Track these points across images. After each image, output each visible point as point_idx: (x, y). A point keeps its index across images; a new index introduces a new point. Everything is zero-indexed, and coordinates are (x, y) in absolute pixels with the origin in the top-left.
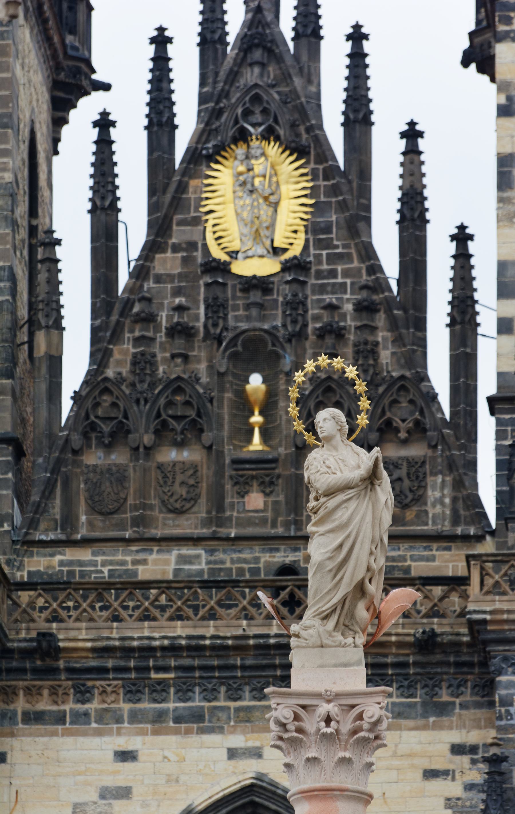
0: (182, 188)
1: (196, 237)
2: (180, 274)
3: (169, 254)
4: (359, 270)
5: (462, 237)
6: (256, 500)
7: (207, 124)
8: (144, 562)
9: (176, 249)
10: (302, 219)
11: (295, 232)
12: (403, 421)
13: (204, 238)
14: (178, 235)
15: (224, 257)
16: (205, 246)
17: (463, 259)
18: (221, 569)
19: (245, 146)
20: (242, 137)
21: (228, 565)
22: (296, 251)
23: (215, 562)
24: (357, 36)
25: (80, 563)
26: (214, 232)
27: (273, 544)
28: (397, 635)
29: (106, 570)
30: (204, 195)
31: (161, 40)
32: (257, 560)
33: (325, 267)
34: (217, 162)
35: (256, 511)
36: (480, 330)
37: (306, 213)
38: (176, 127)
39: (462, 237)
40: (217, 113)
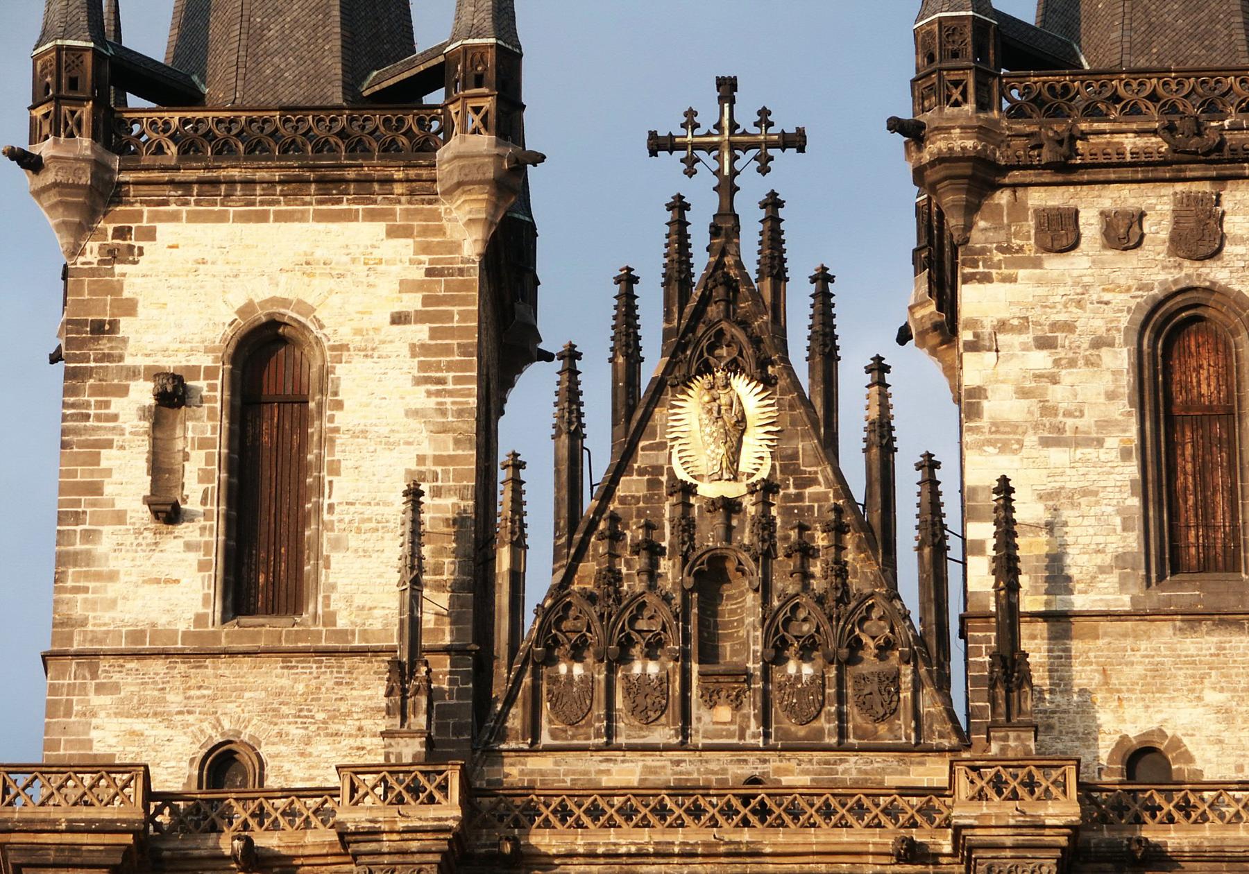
0: (648, 415)
1: (662, 461)
2: (645, 496)
3: (635, 477)
4: (827, 494)
5: (929, 464)
6: (724, 713)
7: (673, 356)
8: (608, 772)
9: (641, 472)
10: (769, 446)
11: (761, 458)
12: (873, 638)
13: (670, 462)
14: (642, 459)
15: (690, 480)
16: (671, 472)
17: (931, 485)
18: (687, 780)
19: (710, 378)
20: (706, 369)
21: (695, 776)
22: (764, 473)
23: (681, 773)
24: (823, 278)
25: (541, 773)
26: (681, 458)
27: (744, 755)
28: (874, 844)
29: (568, 779)
30: (671, 424)
31: (628, 279)
32: (724, 771)
33: (792, 490)
34: (683, 392)
35: (725, 723)
36: (949, 554)
37: (771, 440)
38: (642, 359)
39: (929, 464)
40: (681, 347)
